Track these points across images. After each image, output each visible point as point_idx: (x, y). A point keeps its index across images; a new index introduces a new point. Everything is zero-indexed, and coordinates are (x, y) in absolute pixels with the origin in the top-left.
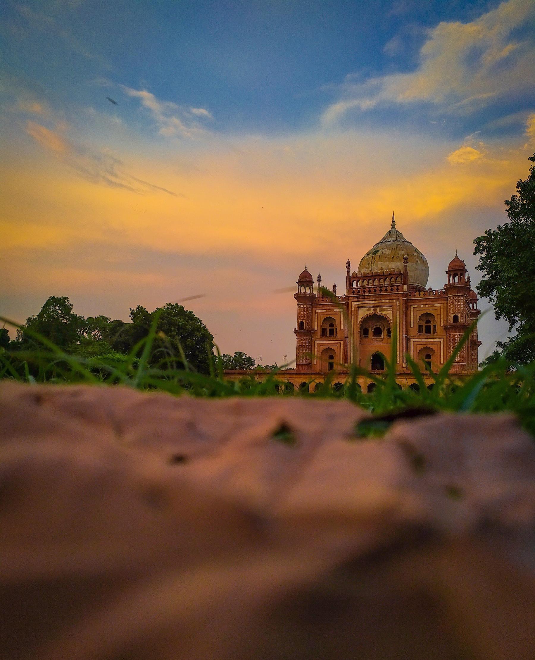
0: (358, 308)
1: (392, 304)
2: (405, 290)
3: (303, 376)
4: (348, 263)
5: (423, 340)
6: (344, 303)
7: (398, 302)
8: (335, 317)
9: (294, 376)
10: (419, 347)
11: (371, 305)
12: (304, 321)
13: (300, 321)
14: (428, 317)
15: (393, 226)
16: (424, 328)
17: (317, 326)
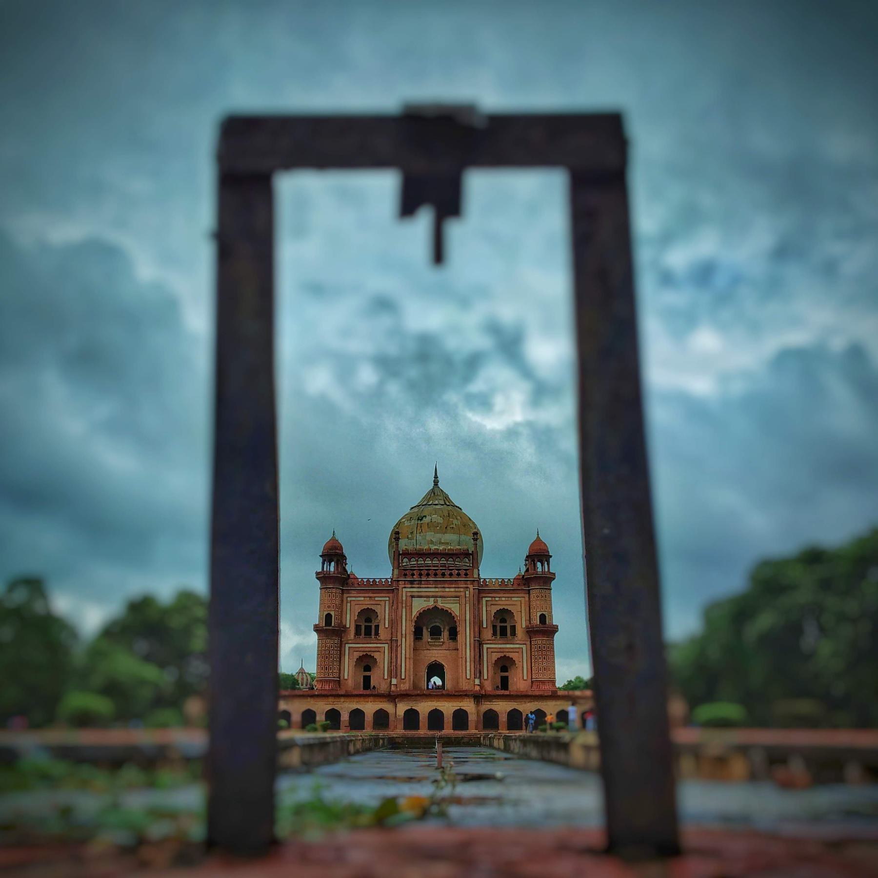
0: (412, 597)
1: (458, 594)
2: (476, 576)
3: (356, 699)
4: (397, 533)
5: (500, 646)
6: (389, 589)
7: (467, 592)
8: (378, 609)
9: (342, 700)
10: (495, 656)
11: (431, 594)
12: (333, 613)
13: (326, 613)
14: (503, 615)
15: (436, 483)
16: (498, 628)
17: (350, 621)
